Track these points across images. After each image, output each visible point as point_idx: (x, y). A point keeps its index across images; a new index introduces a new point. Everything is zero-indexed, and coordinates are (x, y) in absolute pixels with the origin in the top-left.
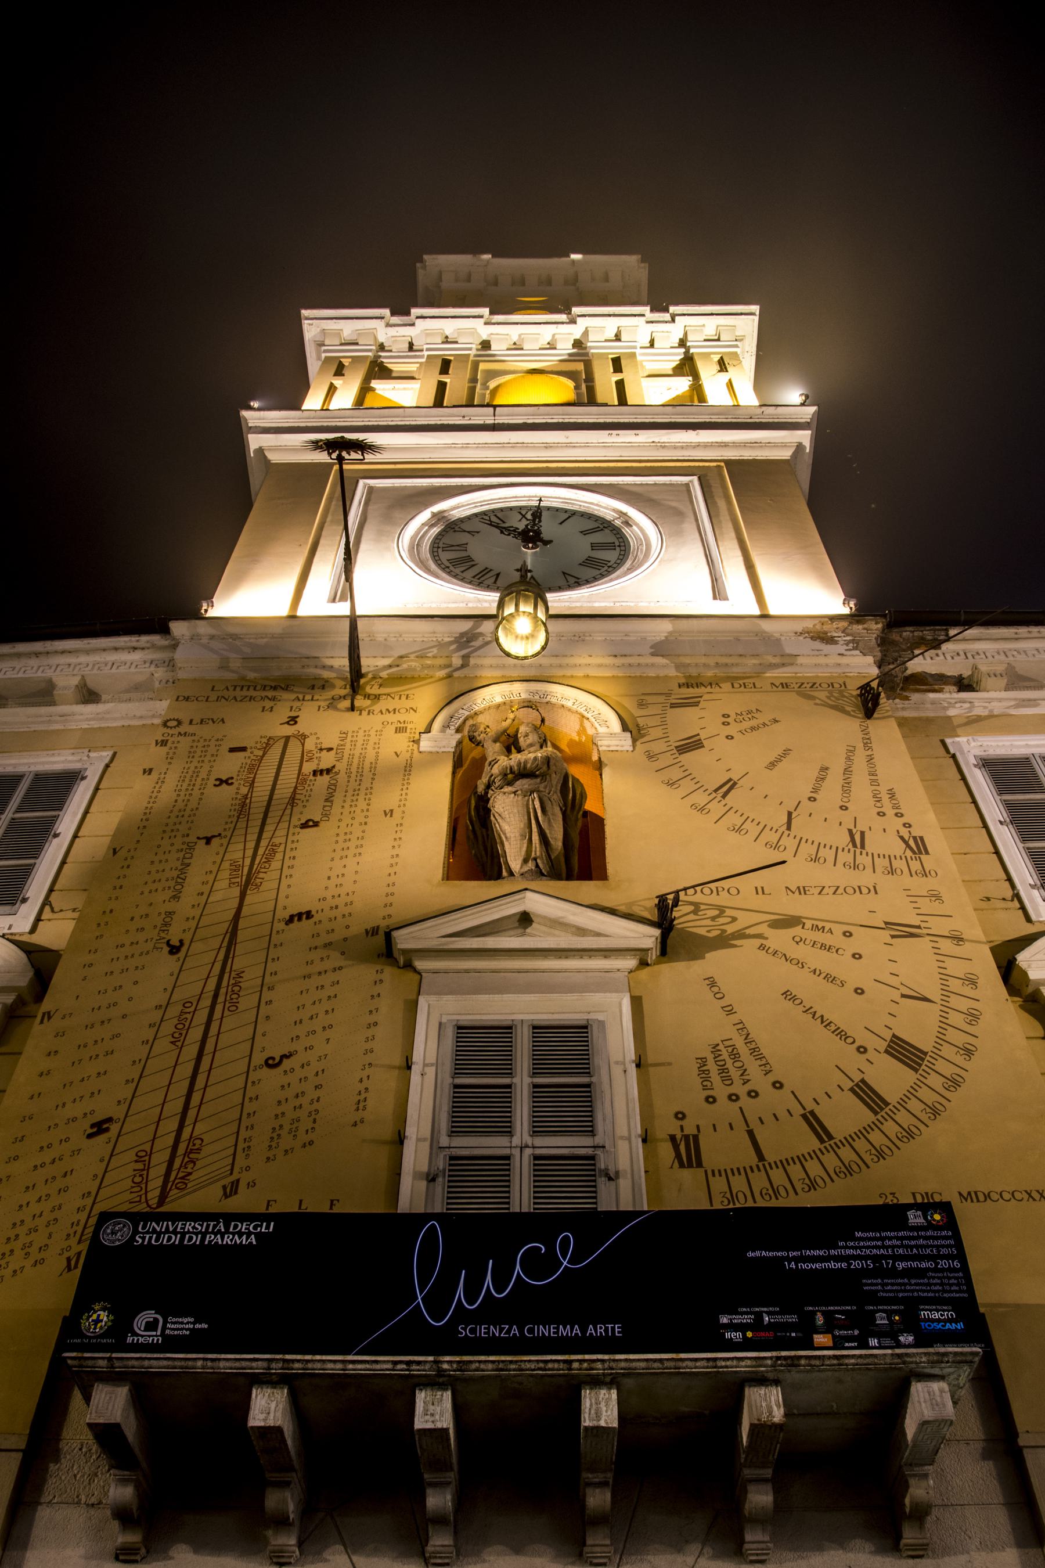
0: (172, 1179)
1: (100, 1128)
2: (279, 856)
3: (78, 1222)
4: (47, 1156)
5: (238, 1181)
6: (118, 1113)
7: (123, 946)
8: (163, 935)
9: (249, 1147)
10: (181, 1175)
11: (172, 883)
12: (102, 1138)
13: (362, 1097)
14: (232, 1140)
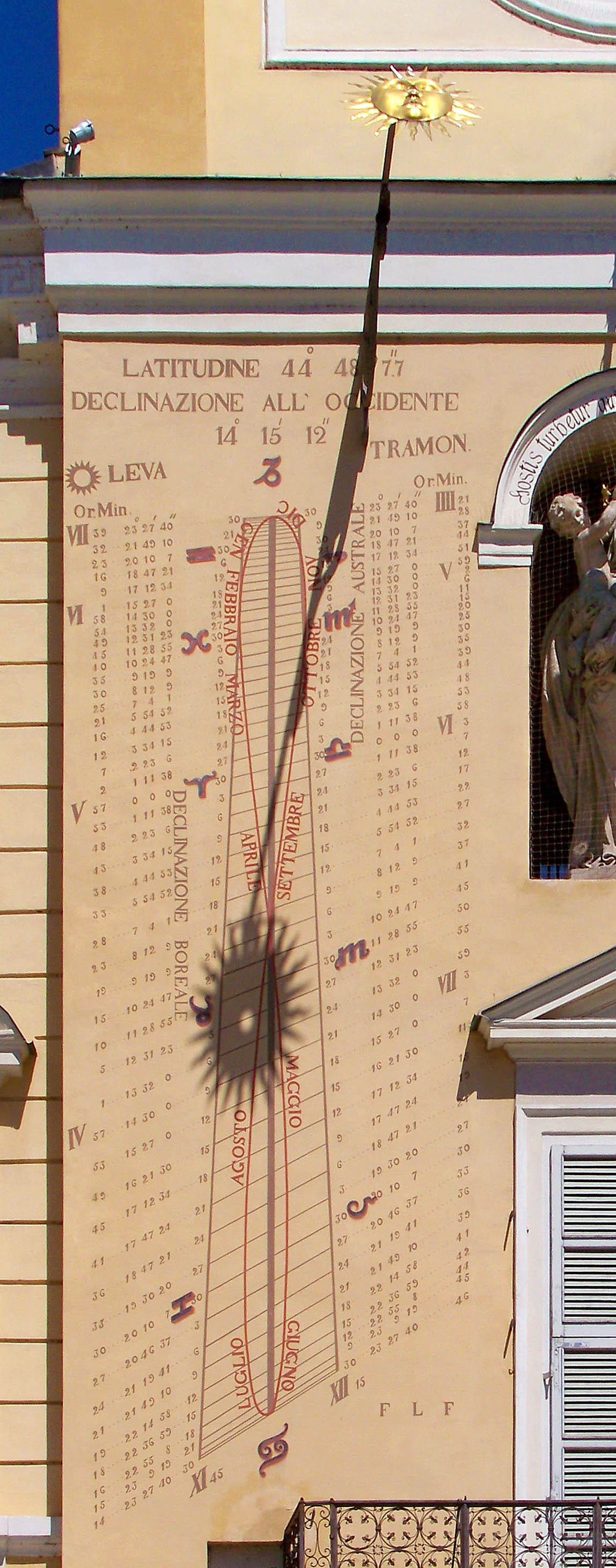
0: (276, 1377)
1: (183, 1308)
2: (305, 820)
3: (192, 1432)
4: (136, 1347)
5: (346, 1378)
6: (197, 1287)
7: (135, 1008)
8: (182, 987)
9: (350, 1333)
10: (285, 1371)
11: (170, 883)
12: (188, 1321)
13: (462, 1262)
14: (328, 1326)
